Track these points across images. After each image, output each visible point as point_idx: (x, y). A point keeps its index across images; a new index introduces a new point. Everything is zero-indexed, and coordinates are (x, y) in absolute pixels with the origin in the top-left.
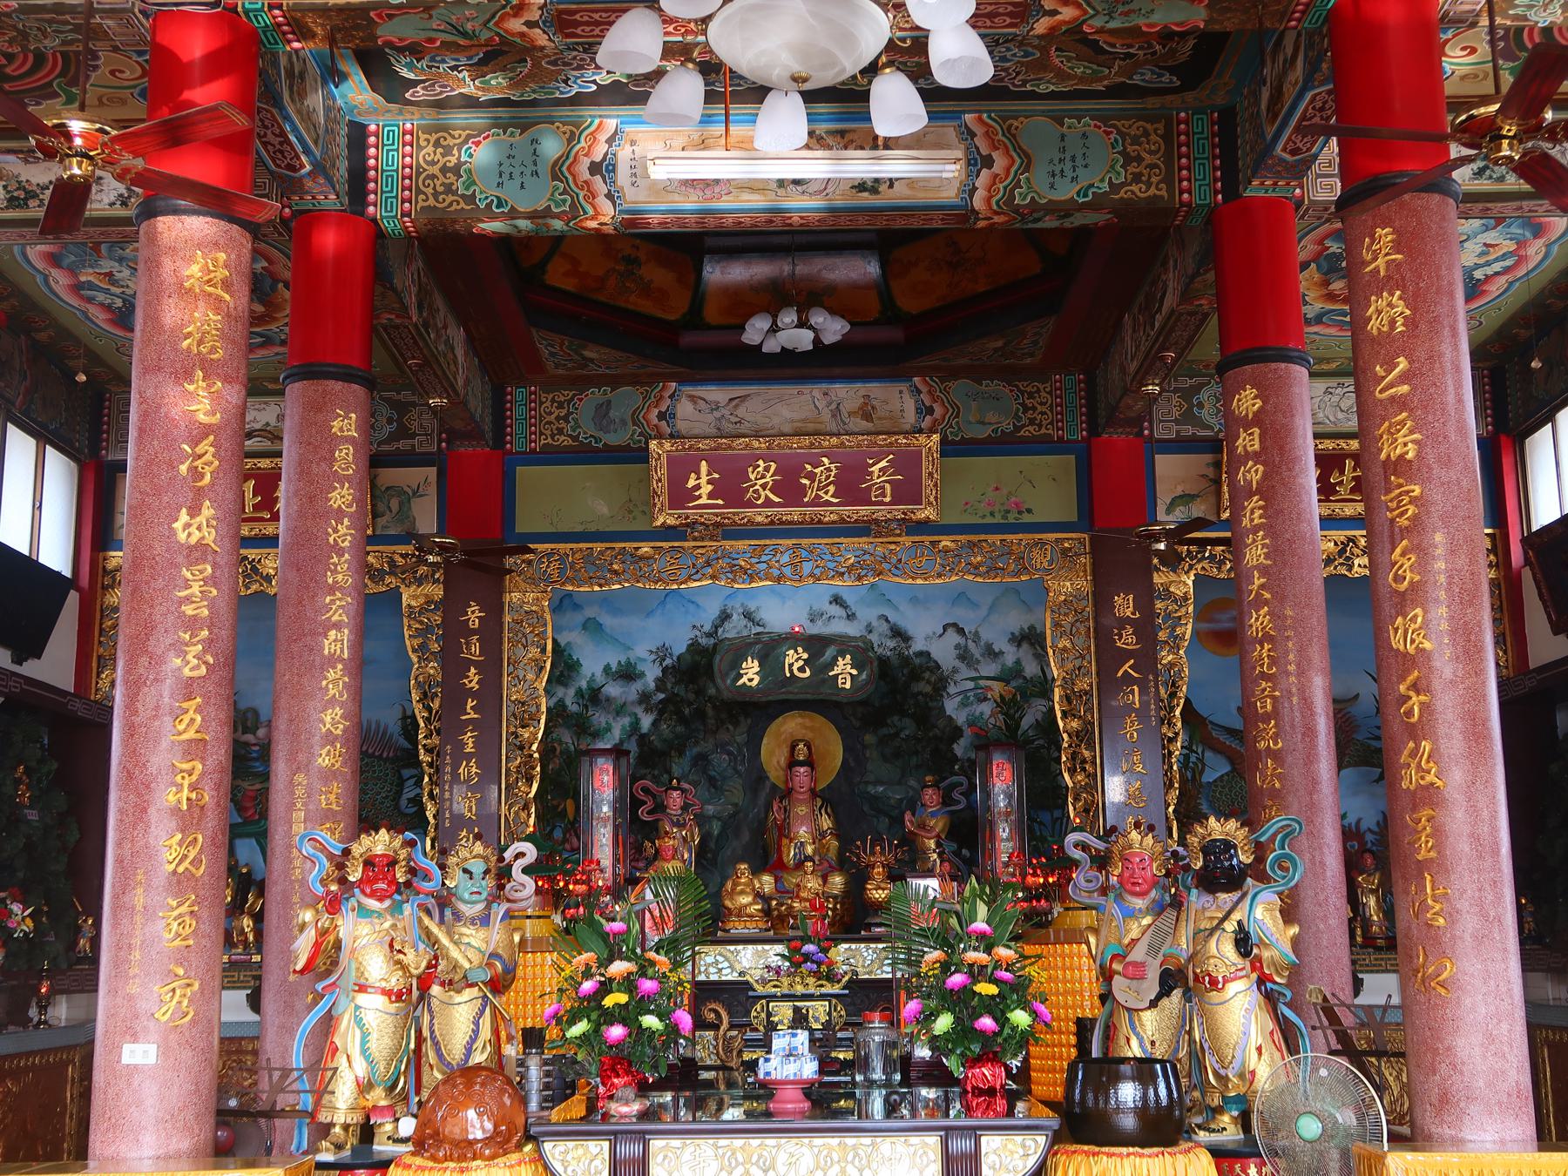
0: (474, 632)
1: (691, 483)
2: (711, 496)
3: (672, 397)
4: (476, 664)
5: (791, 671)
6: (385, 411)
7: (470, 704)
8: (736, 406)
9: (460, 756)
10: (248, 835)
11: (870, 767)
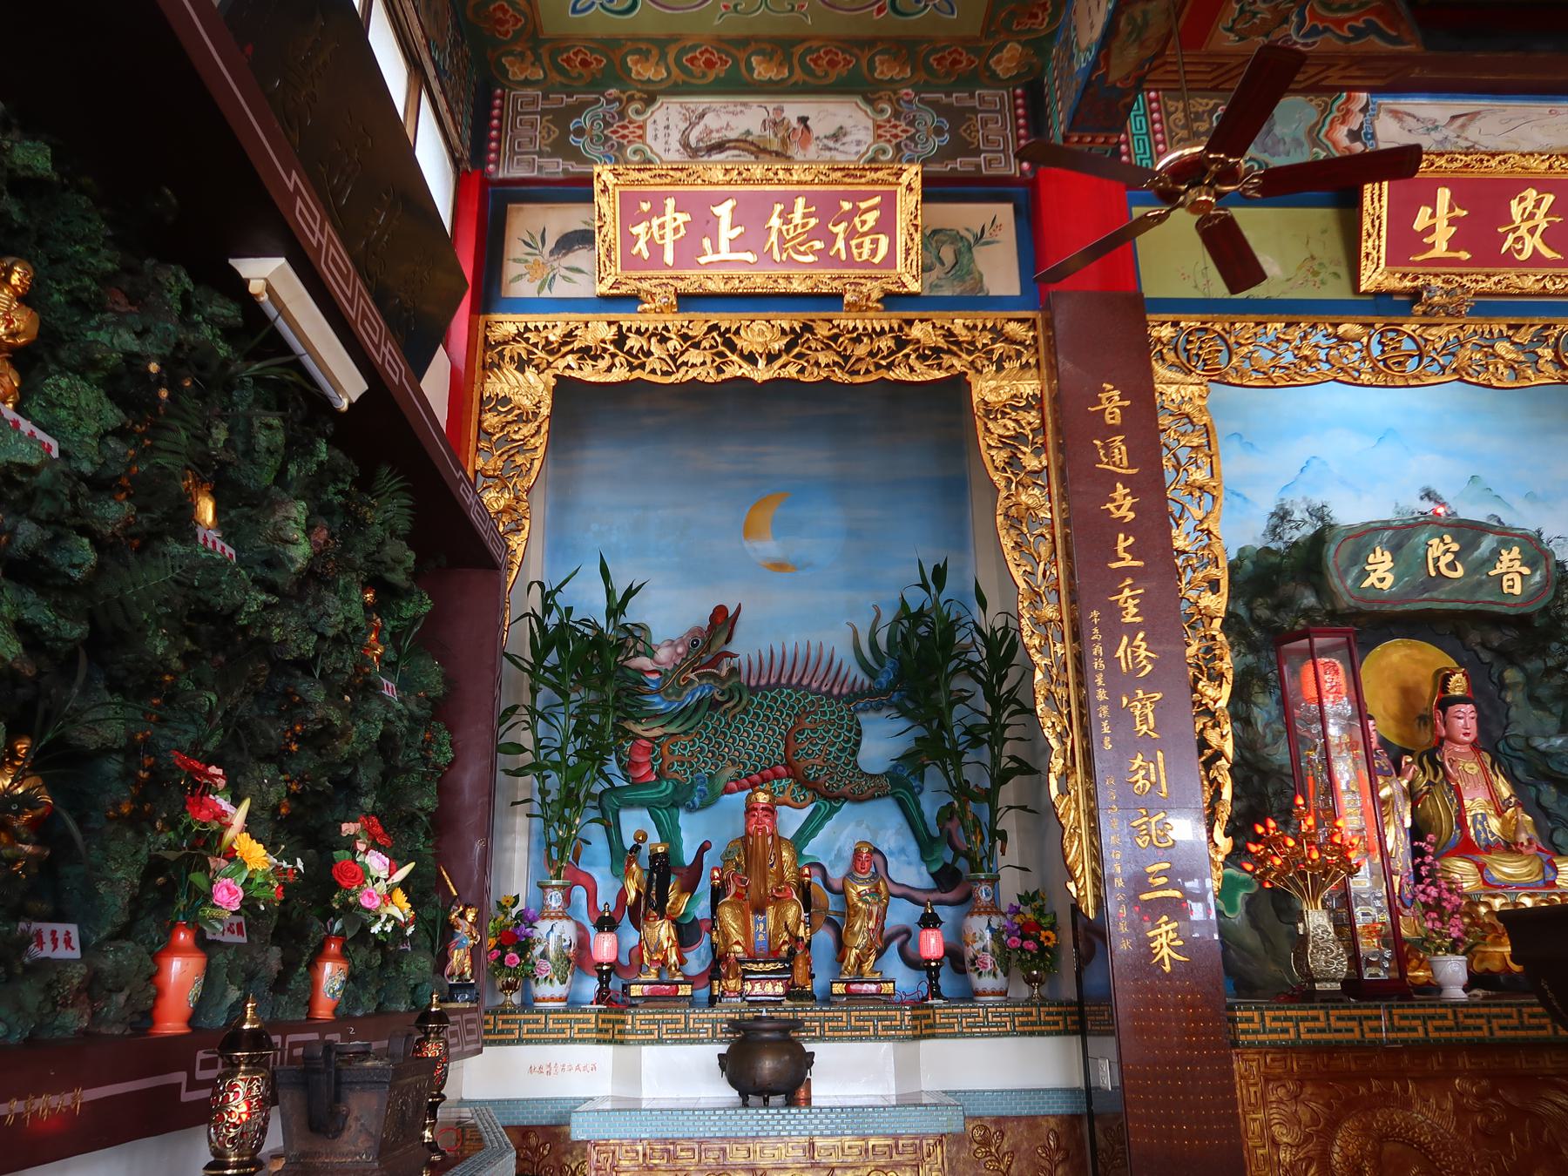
0: (1115, 430)
1: (1421, 221)
2: (1453, 244)
3: (1364, 110)
4: (1127, 481)
5: (1437, 569)
6: (929, 118)
7: (1123, 543)
8: (1463, 126)
9: (1114, 628)
10: (642, 804)
11: (1513, 712)
